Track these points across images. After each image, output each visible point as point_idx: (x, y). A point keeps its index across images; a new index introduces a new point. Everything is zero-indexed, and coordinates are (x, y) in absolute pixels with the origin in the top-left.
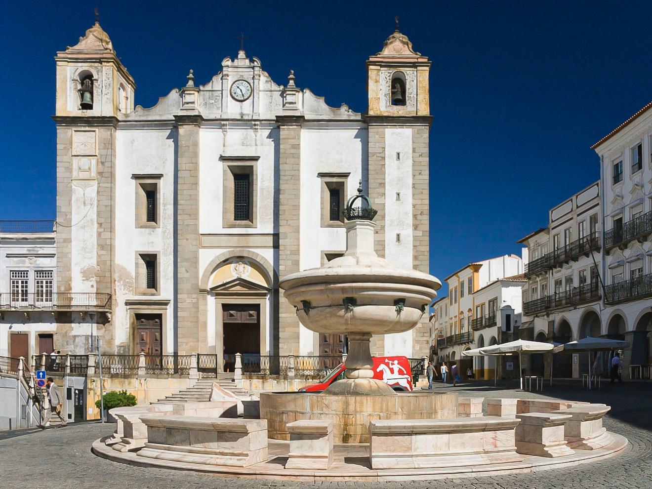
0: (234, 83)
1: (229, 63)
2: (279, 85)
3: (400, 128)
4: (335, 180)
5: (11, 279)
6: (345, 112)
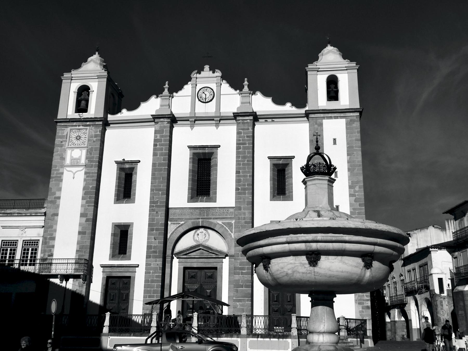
0: (200, 89)
1: (198, 75)
2: (236, 90)
3: (335, 119)
4: (281, 162)
5: (1, 247)
6: (288, 108)
